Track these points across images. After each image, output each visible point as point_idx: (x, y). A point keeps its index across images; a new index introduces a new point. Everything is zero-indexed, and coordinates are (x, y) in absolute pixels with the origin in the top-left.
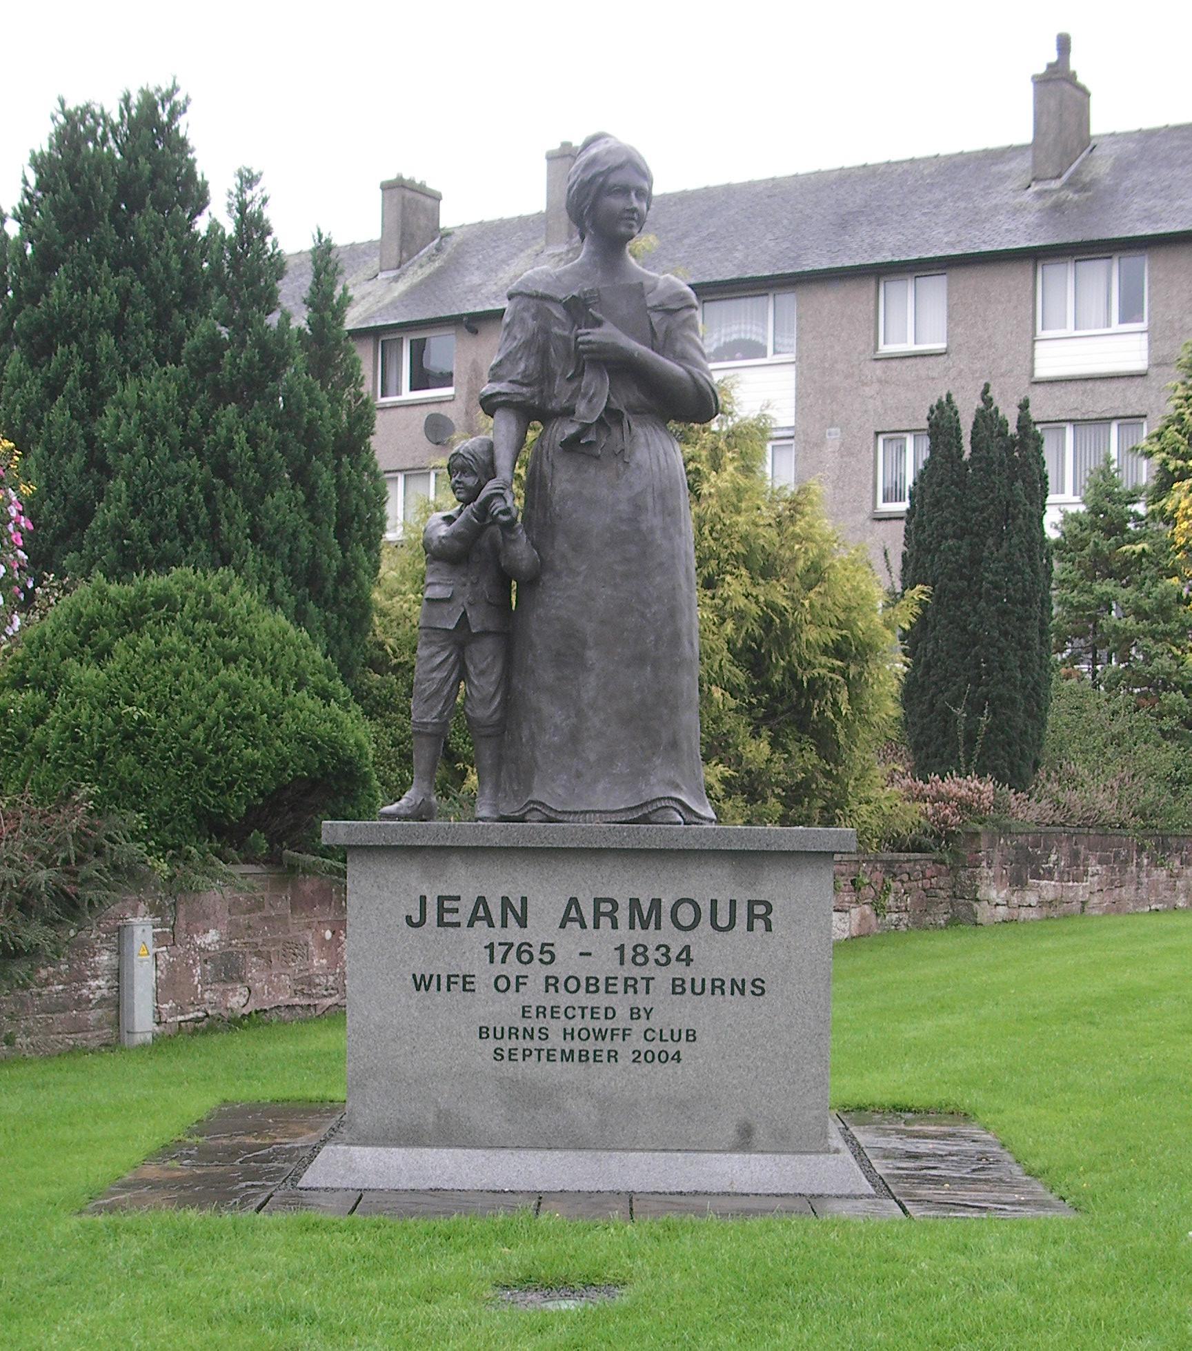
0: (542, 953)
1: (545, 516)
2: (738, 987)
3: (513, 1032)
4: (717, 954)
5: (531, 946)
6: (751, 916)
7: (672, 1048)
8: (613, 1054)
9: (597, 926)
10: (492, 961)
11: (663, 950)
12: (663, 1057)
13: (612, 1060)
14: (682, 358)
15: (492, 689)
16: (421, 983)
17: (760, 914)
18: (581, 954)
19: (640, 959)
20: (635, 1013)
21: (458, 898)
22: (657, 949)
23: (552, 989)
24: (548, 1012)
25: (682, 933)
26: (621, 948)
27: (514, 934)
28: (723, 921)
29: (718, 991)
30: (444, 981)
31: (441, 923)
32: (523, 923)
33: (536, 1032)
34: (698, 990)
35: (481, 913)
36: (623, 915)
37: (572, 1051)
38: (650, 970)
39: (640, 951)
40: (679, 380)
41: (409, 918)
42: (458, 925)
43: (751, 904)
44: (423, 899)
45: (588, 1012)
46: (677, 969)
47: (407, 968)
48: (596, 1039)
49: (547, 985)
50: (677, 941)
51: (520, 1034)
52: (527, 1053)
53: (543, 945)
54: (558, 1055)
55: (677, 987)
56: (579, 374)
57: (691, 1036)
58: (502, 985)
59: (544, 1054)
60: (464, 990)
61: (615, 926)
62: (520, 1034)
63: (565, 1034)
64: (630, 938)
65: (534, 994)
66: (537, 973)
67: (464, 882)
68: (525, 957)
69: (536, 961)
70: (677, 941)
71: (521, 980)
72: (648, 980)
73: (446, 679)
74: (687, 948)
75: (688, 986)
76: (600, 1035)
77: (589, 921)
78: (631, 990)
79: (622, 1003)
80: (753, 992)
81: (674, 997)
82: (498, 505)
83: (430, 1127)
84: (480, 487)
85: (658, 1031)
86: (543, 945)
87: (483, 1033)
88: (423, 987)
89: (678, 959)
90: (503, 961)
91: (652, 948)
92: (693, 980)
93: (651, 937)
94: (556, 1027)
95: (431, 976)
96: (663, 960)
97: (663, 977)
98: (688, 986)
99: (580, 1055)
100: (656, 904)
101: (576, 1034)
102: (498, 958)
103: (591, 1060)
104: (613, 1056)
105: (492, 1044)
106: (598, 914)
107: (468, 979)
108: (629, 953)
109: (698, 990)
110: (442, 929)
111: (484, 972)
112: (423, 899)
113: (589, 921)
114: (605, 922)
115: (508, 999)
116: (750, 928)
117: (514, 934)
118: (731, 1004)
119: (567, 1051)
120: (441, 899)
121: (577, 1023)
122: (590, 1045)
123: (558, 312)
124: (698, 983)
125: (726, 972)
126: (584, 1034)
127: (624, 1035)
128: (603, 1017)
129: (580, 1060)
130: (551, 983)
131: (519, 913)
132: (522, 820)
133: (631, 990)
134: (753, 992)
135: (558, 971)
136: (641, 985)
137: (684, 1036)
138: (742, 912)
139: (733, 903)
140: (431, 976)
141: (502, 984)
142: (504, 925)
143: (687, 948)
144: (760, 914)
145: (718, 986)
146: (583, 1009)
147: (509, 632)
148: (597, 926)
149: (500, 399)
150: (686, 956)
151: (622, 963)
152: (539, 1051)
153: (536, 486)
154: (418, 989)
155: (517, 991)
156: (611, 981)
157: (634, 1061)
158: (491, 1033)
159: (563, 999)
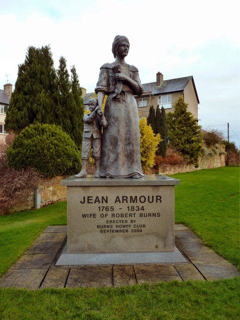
2: (154, 215)
3: (105, 226)
4: (150, 208)
6: (157, 199)
7: (140, 229)
12: (138, 231)
14: (136, 81)
16: (84, 216)
17: (159, 199)
20: (132, 221)
27: (105, 205)
28: (151, 200)
31: (88, 202)
32: (106, 202)
35: (97, 200)
36: (129, 200)
39: (133, 208)
40: (135, 86)
43: (157, 197)
44: (84, 197)
46: (141, 211)
50: (141, 205)
55: (141, 215)
56: (116, 84)
57: (144, 226)
58: (102, 216)
65: (109, 218)
66: (110, 213)
67: (94, 193)
70: (141, 205)
75: (143, 215)
76: (124, 226)
79: (129, 219)
82: (99, 111)
87: (98, 227)
93: (135, 205)
94: (114, 225)
97: (138, 213)
98: (143, 215)
100: (136, 197)
105: (100, 229)
106: (123, 200)
108: (130, 208)
111: (98, 214)
112: (84, 197)
116: (157, 202)
117: (105, 205)
118: (152, 218)
120: (88, 197)
121: (119, 224)
122: (122, 229)
123: (111, 71)
125: (152, 212)
130: (113, 215)
135: (115, 212)
136: (133, 215)
138: (155, 198)
141: (102, 216)
142: (102, 202)
144: (159, 199)
150: (143, 209)
153: (107, 108)
159: (116, 219)
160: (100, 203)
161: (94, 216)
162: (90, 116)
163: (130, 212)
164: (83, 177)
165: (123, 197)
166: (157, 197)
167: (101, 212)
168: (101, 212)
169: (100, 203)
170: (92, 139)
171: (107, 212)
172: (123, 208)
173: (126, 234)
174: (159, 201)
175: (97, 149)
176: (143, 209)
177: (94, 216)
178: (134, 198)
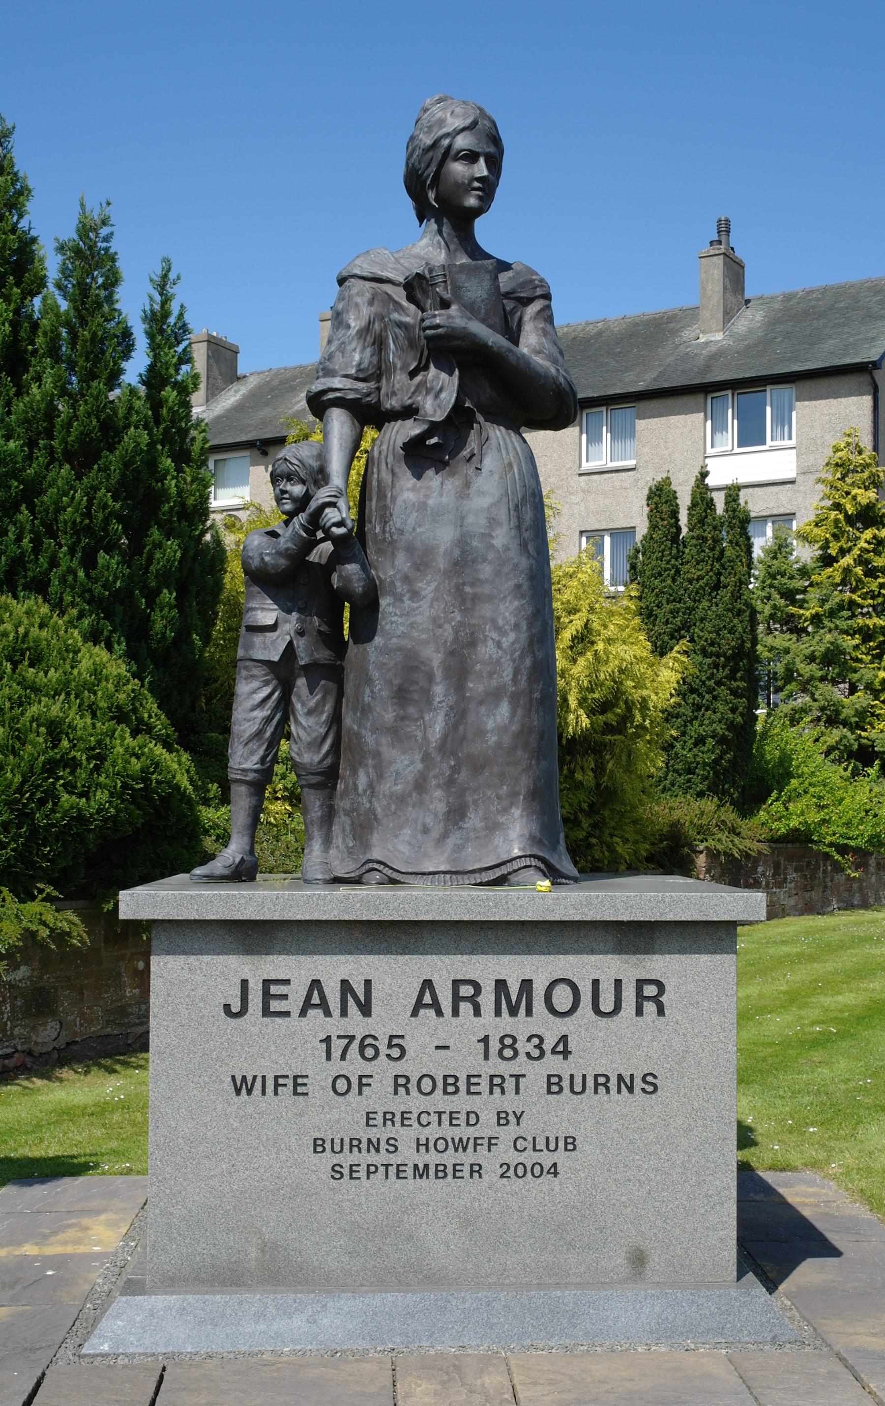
0: (390, 1046)
1: (384, 531)
2: (626, 1084)
3: (355, 1144)
4: (600, 1044)
5: (375, 1038)
6: (641, 998)
8: (476, 1168)
9: (456, 1012)
10: (329, 1058)
11: (536, 1041)
12: (537, 1171)
13: (476, 1175)
15: (323, 731)
16: (242, 1086)
17: (651, 996)
18: (437, 1048)
19: (508, 1053)
20: (502, 1118)
21: (287, 982)
22: (529, 1039)
23: (402, 1090)
24: (398, 1119)
25: (558, 1020)
26: (485, 1040)
28: (607, 1005)
29: (602, 1089)
30: (270, 1083)
31: (266, 1012)
32: (366, 1009)
33: (383, 1144)
34: (578, 1088)
35: (316, 1000)
36: (487, 999)
37: (426, 1166)
38: (521, 1065)
39: (508, 1043)
41: (227, 1008)
42: (287, 1014)
43: (640, 984)
44: (244, 983)
45: (445, 1118)
46: (553, 1064)
47: (224, 1068)
48: (456, 1150)
49: (396, 1086)
50: (551, 1030)
51: (364, 1146)
52: (372, 1169)
53: (392, 1037)
54: (410, 1171)
55: (553, 1085)
57: (570, 1144)
58: (341, 1087)
59: (392, 1170)
60: (295, 1093)
61: (477, 1012)
62: (364, 1146)
63: (418, 1145)
64: (496, 1027)
65: (380, 1096)
66: (383, 1071)
68: (369, 1052)
69: (382, 1057)
70: (551, 1030)
71: (364, 1081)
72: (518, 1077)
73: (268, 720)
74: (564, 1039)
75: (566, 1084)
76: (461, 1145)
77: (446, 1004)
78: (497, 1090)
79: (487, 1105)
80: (643, 1090)
81: (551, 1097)
82: (331, 515)
83: (253, 1263)
84: (307, 498)
85: (530, 1139)
86: (392, 1037)
87: (318, 1145)
88: (244, 1091)
89: (554, 1052)
90: (343, 1057)
91: (521, 1039)
92: (572, 1076)
93: (520, 1026)
94: (406, 1137)
95: (255, 1077)
96: (536, 1053)
97: (536, 1074)
98: (566, 1084)
99: (437, 1171)
100: (527, 985)
101: (431, 1144)
102: (336, 1053)
103: (450, 1176)
104: (476, 1170)
105: (328, 1159)
106: (457, 999)
107: (300, 1081)
108: (494, 1045)
109: (578, 1088)
110: (267, 1020)
111: (320, 1073)
112: (244, 983)
113: (446, 1004)
114: (466, 1008)
115: (349, 1104)
116: (639, 1012)
118: (617, 1102)
119: (421, 1166)
120: (267, 983)
121: (432, 1132)
122: (450, 1158)
123: (399, 295)
124: (578, 1081)
126: (441, 1145)
127: (490, 1145)
128: (463, 1124)
129: (437, 1177)
130: (401, 1083)
131: (362, 999)
132: (357, 881)
133: (497, 1090)
134: (643, 1090)
135: (411, 1067)
136: (510, 1084)
137: (561, 1144)
139: (618, 983)
140: (255, 1077)
141: (342, 1085)
142: (344, 1013)
143: (564, 1039)
144: (651, 996)
145: (601, 1083)
146: (440, 1114)
147: (332, 673)
148: (456, 1012)
149: (331, 395)
150: (563, 1048)
151: (486, 1057)
152: (387, 1166)
154: (238, 1092)
155: (360, 1093)
156: (473, 1080)
157: (502, 1176)
158: (328, 1146)
159: (415, 1103)
160: (328, 1013)
161: (298, 1082)
162: (284, 543)
163: (496, 1066)
164: (243, 873)
165: (456, 983)
166: (640, 984)
167: (337, 1067)
168: (337, 1067)
169: (328, 1013)
170: (283, 671)
171: (366, 1068)
172: (453, 1042)
173: (468, 1186)
174: (650, 1008)
175: (308, 724)
176: (566, 1053)
177: (298, 1082)
178: (514, 989)
